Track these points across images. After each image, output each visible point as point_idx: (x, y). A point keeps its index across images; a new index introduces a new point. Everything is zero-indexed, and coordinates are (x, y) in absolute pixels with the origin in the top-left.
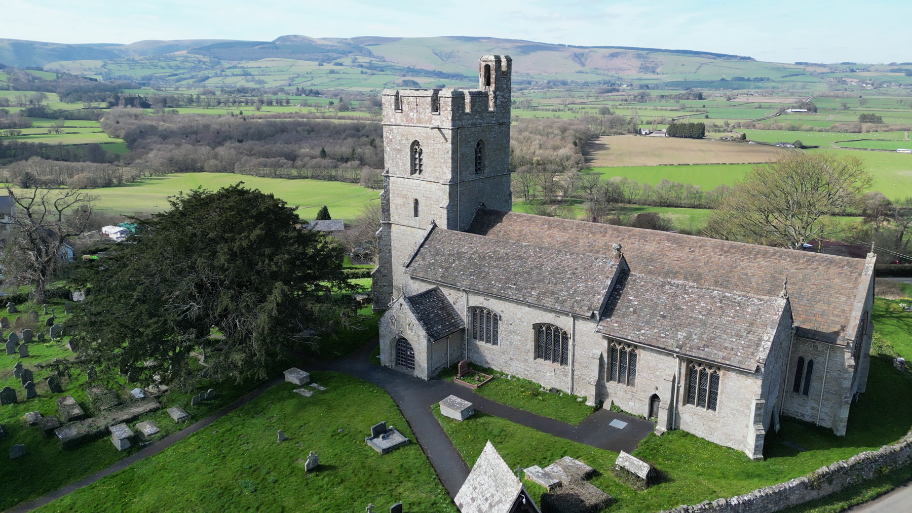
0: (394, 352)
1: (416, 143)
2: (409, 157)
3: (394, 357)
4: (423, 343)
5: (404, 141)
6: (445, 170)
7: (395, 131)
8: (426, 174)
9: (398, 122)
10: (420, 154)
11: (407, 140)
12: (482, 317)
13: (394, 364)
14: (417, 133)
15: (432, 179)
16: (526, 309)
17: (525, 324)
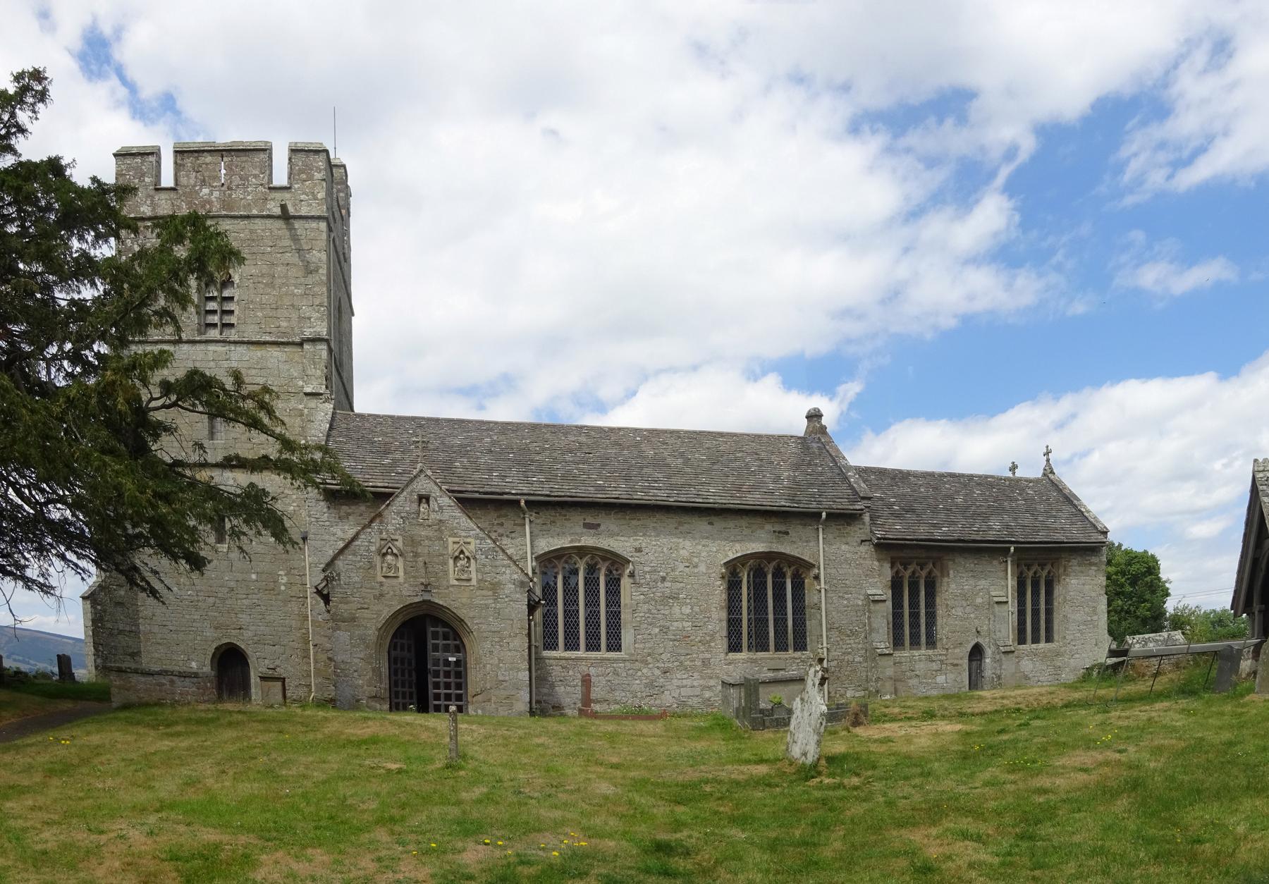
17: (702, 568)
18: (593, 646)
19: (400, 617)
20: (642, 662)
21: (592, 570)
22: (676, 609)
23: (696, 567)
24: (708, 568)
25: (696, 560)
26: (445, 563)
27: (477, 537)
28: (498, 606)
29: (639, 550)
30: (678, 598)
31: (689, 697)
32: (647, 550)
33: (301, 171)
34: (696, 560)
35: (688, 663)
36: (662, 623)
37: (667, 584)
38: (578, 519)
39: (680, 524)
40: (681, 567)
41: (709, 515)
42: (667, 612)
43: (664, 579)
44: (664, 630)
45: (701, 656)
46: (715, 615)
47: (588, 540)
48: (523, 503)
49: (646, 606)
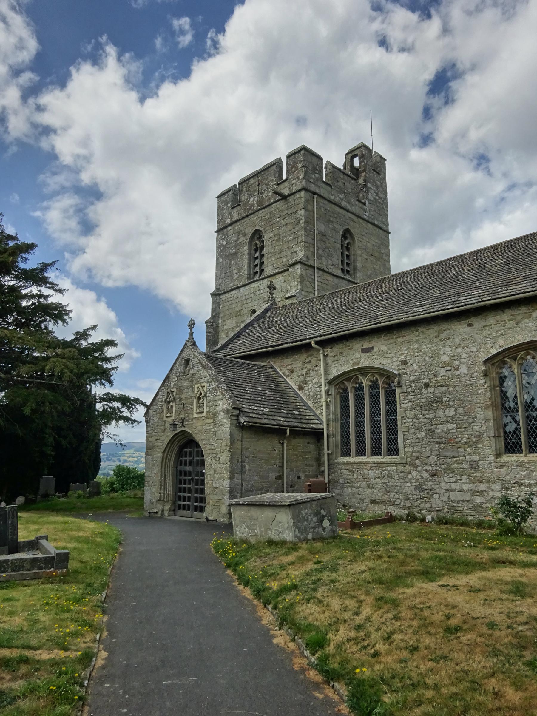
0: (170, 480)
1: (257, 234)
2: (246, 258)
3: (169, 491)
4: (225, 427)
5: (242, 239)
6: (295, 248)
7: (231, 233)
8: (268, 270)
9: (234, 220)
10: (262, 247)
11: (245, 235)
12: (359, 399)
13: (167, 507)
14: (256, 221)
15: (277, 271)
16: (461, 329)
17: (464, 369)
18: (376, 452)
19: (176, 442)
20: (411, 465)
21: (374, 385)
22: (440, 413)
23: (457, 369)
24: (469, 368)
25: (457, 363)
26: (192, 403)
27: (209, 382)
28: (216, 429)
29: (404, 363)
30: (441, 402)
31: (459, 502)
32: (411, 362)
33: (293, 167)
34: (457, 363)
35: (455, 466)
36: (427, 427)
37: (431, 390)
38: (357, 345)
39: (440, 332)
40: (442, 372)
41: (468, 317)
42: (431, 416)
43: (427, 385)
44: (430, 433)
45: (468, 458)
46: (480, 415)
47: (365, 362)
48: (313, 344)
49: (413, 412)
